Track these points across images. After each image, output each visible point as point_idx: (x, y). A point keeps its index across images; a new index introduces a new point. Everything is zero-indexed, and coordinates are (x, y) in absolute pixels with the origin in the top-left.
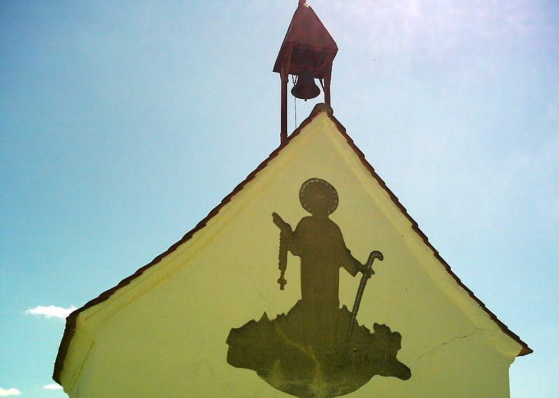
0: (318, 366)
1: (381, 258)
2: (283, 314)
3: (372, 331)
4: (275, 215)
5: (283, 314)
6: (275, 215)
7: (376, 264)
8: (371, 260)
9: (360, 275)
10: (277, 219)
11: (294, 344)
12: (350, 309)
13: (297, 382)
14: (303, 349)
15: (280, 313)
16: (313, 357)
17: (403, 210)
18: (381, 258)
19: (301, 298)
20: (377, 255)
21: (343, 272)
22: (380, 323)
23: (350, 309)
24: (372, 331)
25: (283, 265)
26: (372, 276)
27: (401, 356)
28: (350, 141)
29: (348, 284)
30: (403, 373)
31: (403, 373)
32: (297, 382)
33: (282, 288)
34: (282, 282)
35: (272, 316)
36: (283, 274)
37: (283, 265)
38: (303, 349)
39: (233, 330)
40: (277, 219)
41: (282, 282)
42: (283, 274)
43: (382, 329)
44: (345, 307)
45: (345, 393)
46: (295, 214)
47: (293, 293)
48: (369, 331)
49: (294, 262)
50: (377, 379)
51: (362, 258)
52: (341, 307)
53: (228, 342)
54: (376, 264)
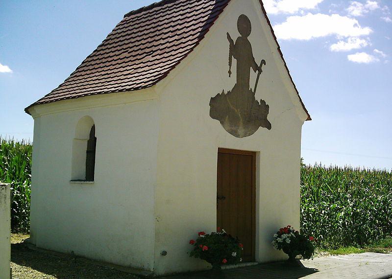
0: (241, 120)
8: (261, 65)
11: (234, 108)
13: (234, 128)
17: (275, 38)
25: (230, 64)
29: (253, 75)
30: (269, 126)
31: (269, 126)
32: (234, 128)
33: (230, 76)
34: (230, 72)
35: (226, 92)
36: (230, 68)
37: (230, 64)
41: (230, 72)
42: (230, 68)
43: (263, 102)
46: (235, 35)
49: (234, 61)
52: (250, 89)
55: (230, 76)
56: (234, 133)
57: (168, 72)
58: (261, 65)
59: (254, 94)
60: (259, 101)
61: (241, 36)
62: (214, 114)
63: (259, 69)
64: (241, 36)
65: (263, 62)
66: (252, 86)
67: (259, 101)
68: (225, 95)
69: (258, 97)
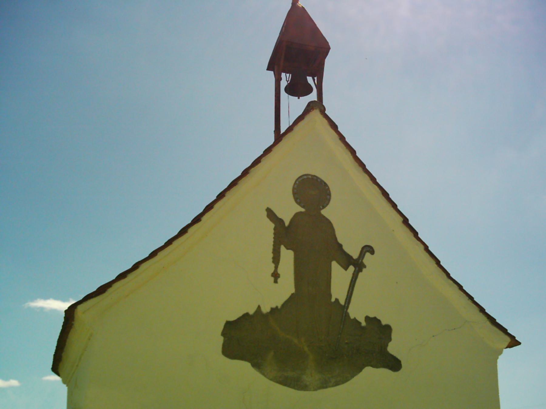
1: (372, 252)
2: (277, 307)
3: (364, 324)
5: (277, 307)
7: (368, 259)
8: (362, 254)
9: (351, 269)
10: (271, 214)
12: (342, 302)
14: (296, 341)
15: (274, 306)
16: (306, 349)
17: (394, 206)
18: (372, 252)
20: (368, 249)
21: (335, 266)
22: (371, 316)
23: (342, 302)
24: (364, 324)
25: (276, 260)
26: (364, 270)
27: (392, 348)
28: (342, 138)
33: (276, 282)
34: (276, 276)
35: (266, 309)
36: (276, 268)
37: (276, 260)
38: (296, 341)
39: (229, 324)
40: (271, 214)
41: (276, 276)
42: (276, 268)
43: (373, 321)
44: (337, 300)
45: (337, 384)
50: (368, 371)
51: (355, 254)
52: (333, 300)
53: (223, 334)
54: (368, 259)
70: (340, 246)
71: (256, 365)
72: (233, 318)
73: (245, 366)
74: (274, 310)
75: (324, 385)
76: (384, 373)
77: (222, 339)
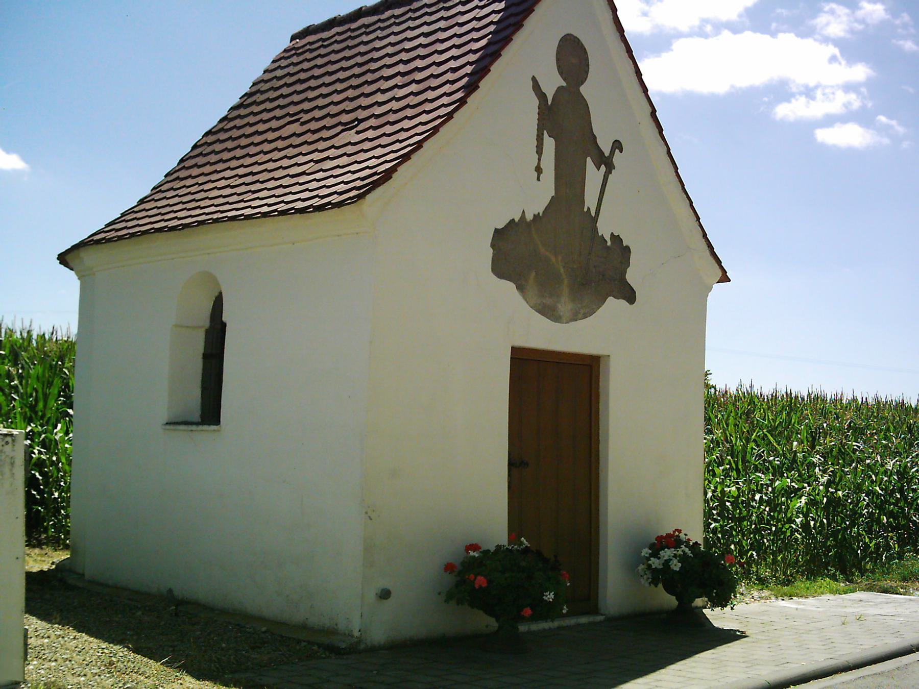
0: (566, 282)
4: (534, 79)
6: (534, 79)
8: (612, 153)
9: (603, 168)
11: (548, 254)
13: (548, 301)
14: (553, 259)
15: (536, 213)
16: (562, 270)
17: (645, 90)
19: (554, 195)
20: (617, 145)
24: (609, 243)
25: (540, 150)
29: (593, 175)
30: (629, 295)
31: (629, 295)
32: (548, 301)
33: (538, 179)
34: (539, 170)
35: (529, 217)
36: (539, 160)
37: (540, 150)
38: (553, 259)
39: (497, 231)
41: (539, 170)
42: (539, 160)
43: (616, 239)
46: (552, 83)
47: (546, 189)
48: (606, 242)
49: (549, 144)
51: (606, 148)
52: (586, 210)
53: (493, 246)
54: (617, 158)
55: (538, 179)
56: (548, 312)
57: (393, 170)
58: (612, 153)
59: (595, 220)
60: (608, 238)
61: (564, 84)
62: (501, 268)
63: (606, 162)
64: (564, 84)
65: (617, 145)
66: (590, 202)
67: (608, 238)
68: (528, 224)
69: (605, 229)
70: (595, 137)
71: (520, 288)
72: (501, 226)
73: (510, 286)
74: (536, 217)
75: (575, 317)
76: (623, 303)
77: (490, 252)
